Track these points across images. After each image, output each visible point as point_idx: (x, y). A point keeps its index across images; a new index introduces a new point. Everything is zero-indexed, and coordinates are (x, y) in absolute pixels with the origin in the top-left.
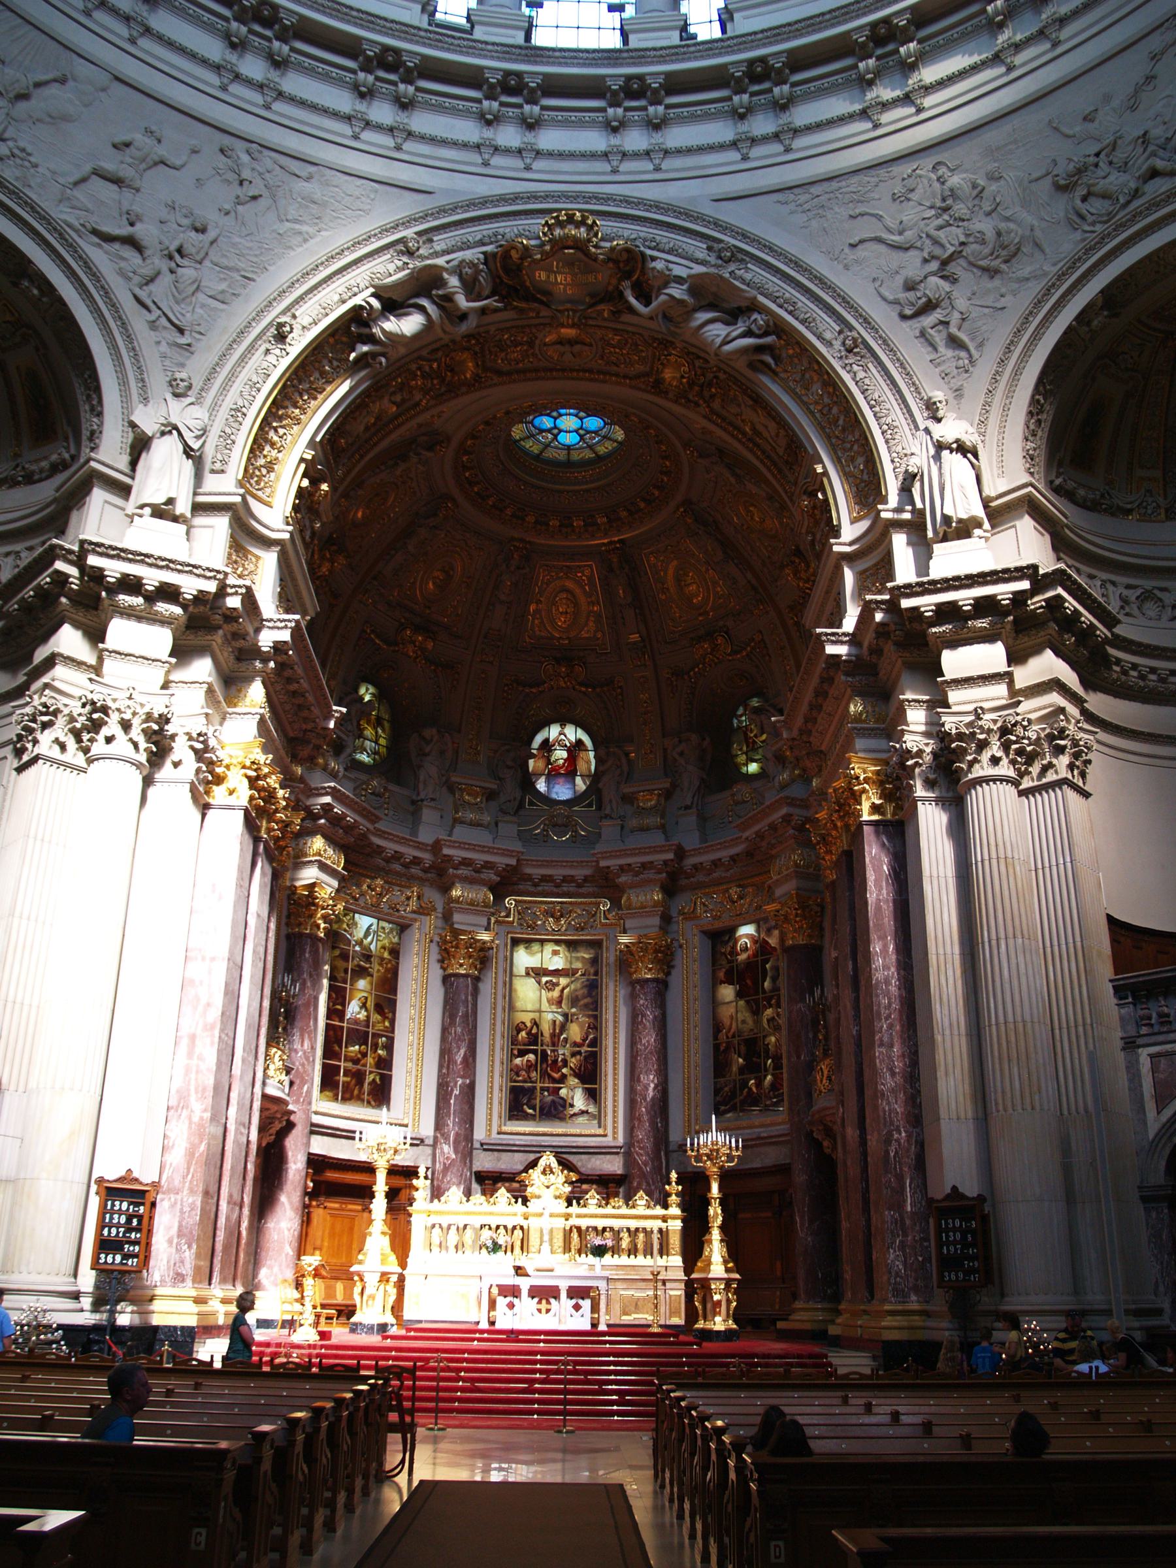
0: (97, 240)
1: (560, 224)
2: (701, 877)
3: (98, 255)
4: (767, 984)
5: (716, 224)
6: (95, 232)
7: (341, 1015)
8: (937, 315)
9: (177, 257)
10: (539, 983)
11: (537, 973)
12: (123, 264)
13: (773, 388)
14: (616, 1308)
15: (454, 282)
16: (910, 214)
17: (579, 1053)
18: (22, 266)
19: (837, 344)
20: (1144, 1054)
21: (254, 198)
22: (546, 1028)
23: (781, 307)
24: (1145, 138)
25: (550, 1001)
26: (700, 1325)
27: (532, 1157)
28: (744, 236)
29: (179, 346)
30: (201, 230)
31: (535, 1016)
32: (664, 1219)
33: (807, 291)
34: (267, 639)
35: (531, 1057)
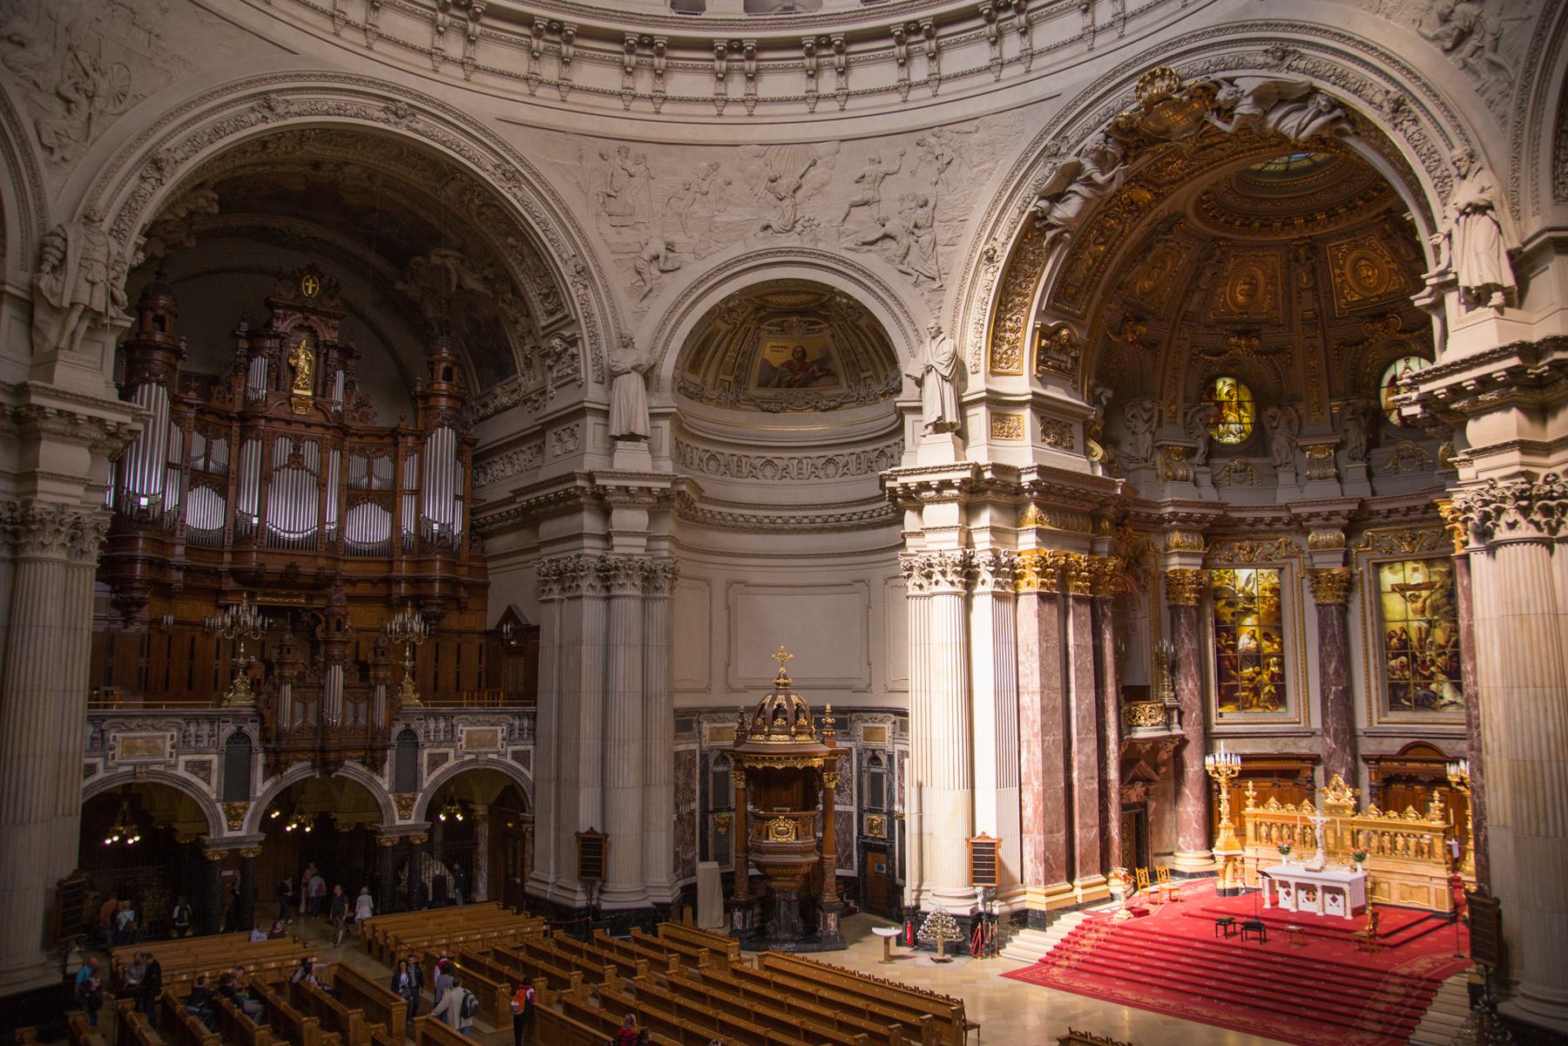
0: (866, 248)
1: (1152, 82)
5: (1268, 25)
6: (864, 244)
7: (1234, 648)
8: (1472, 43)
9: (916, 231)
10: (1404, 597)
11: (1402, 589)
12: (887, 253)
15: (1088, 166)
17: (1444, 653)
18: (831, 289)
19: (1387, 107)
21: (949, 163)
22: (1414, 635)
23: (1335, 84)
25: (1414, 612)
27: (1410, 741)
29: (935, 290)
30: (926, 204)
31: (1404, 624)
33: (1354, 59)
34: (1026, 480)
35: (1404, 659)
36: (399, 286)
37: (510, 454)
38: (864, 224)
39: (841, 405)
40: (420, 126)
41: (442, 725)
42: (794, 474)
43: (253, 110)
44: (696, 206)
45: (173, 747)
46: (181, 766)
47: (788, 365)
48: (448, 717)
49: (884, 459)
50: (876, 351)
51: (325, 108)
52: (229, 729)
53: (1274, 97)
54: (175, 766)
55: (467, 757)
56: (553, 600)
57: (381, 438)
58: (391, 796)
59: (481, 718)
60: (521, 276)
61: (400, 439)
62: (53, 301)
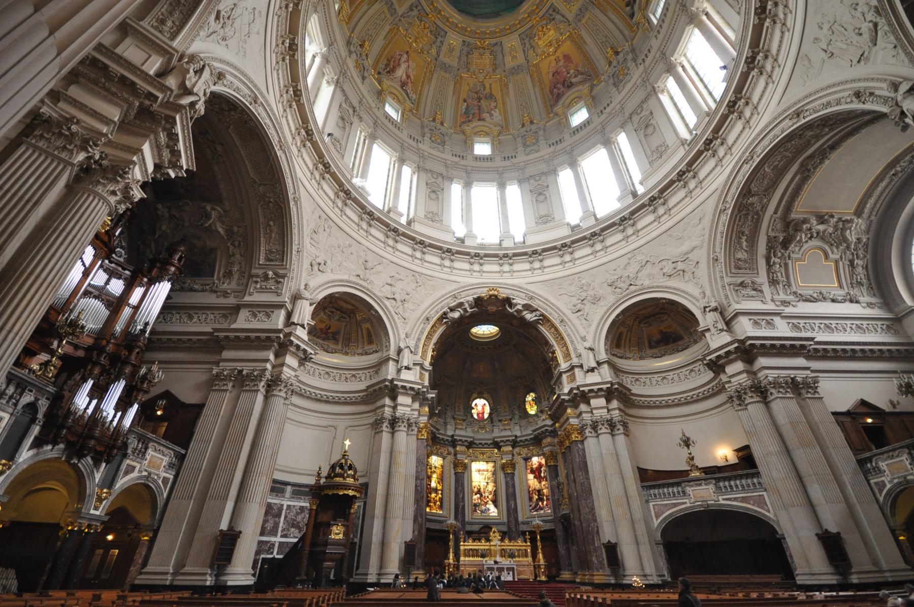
2: (522, 444)
3: (387, 303)
4: (542, 475)
5: (527, 290)
7: (430, 485)
11: (479, 471)
13: (543, 329)
14: (518, 575)
15: (467, 305)
16: (573, 288)
18: (372, 307)
20: (651, 504)
24: (628, 276)
26: (538, 579)
27: (481, 526)
28: (534, 293)
32: (526, 546)
35: (478, 495)
37: (209, 313)
38: (387, 291)
39: (336, 352)
42: (311, 373)
44: (338, 255)
47: (321, 330)
49: (354, 378)
50: (363, 338)
52: (27, 398)
53: (527, 307)
56: (227, 390)
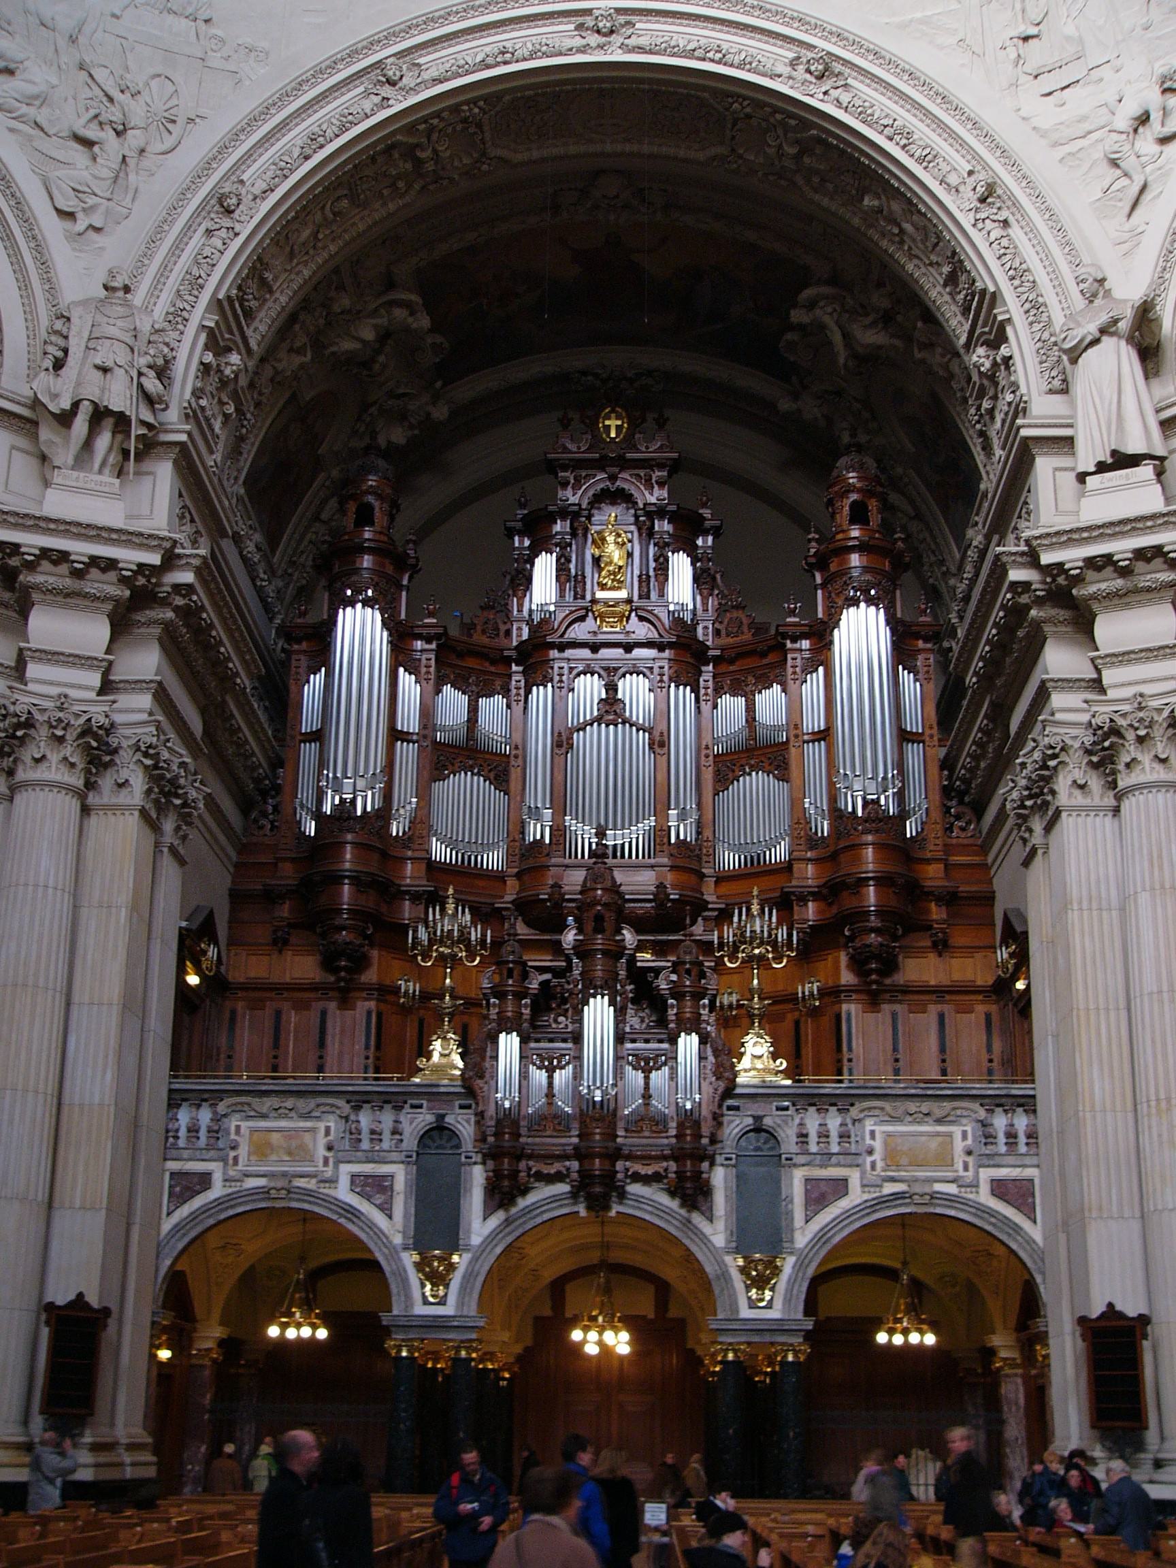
36: (785, 405)
40: (643, 41)
41: (834, 1122)
43: (367, 94)
45: (330, 1148)
46: (344, 1181)
48: (843, 1102)
51: (479, 59)
54: (333, 1181)
55: (889, 1188)
57: (763, 655)
58: (728, 1259)
59: (912, 1106)
60: (910, 267)
61: (789, 645)
62: (53, 407)
